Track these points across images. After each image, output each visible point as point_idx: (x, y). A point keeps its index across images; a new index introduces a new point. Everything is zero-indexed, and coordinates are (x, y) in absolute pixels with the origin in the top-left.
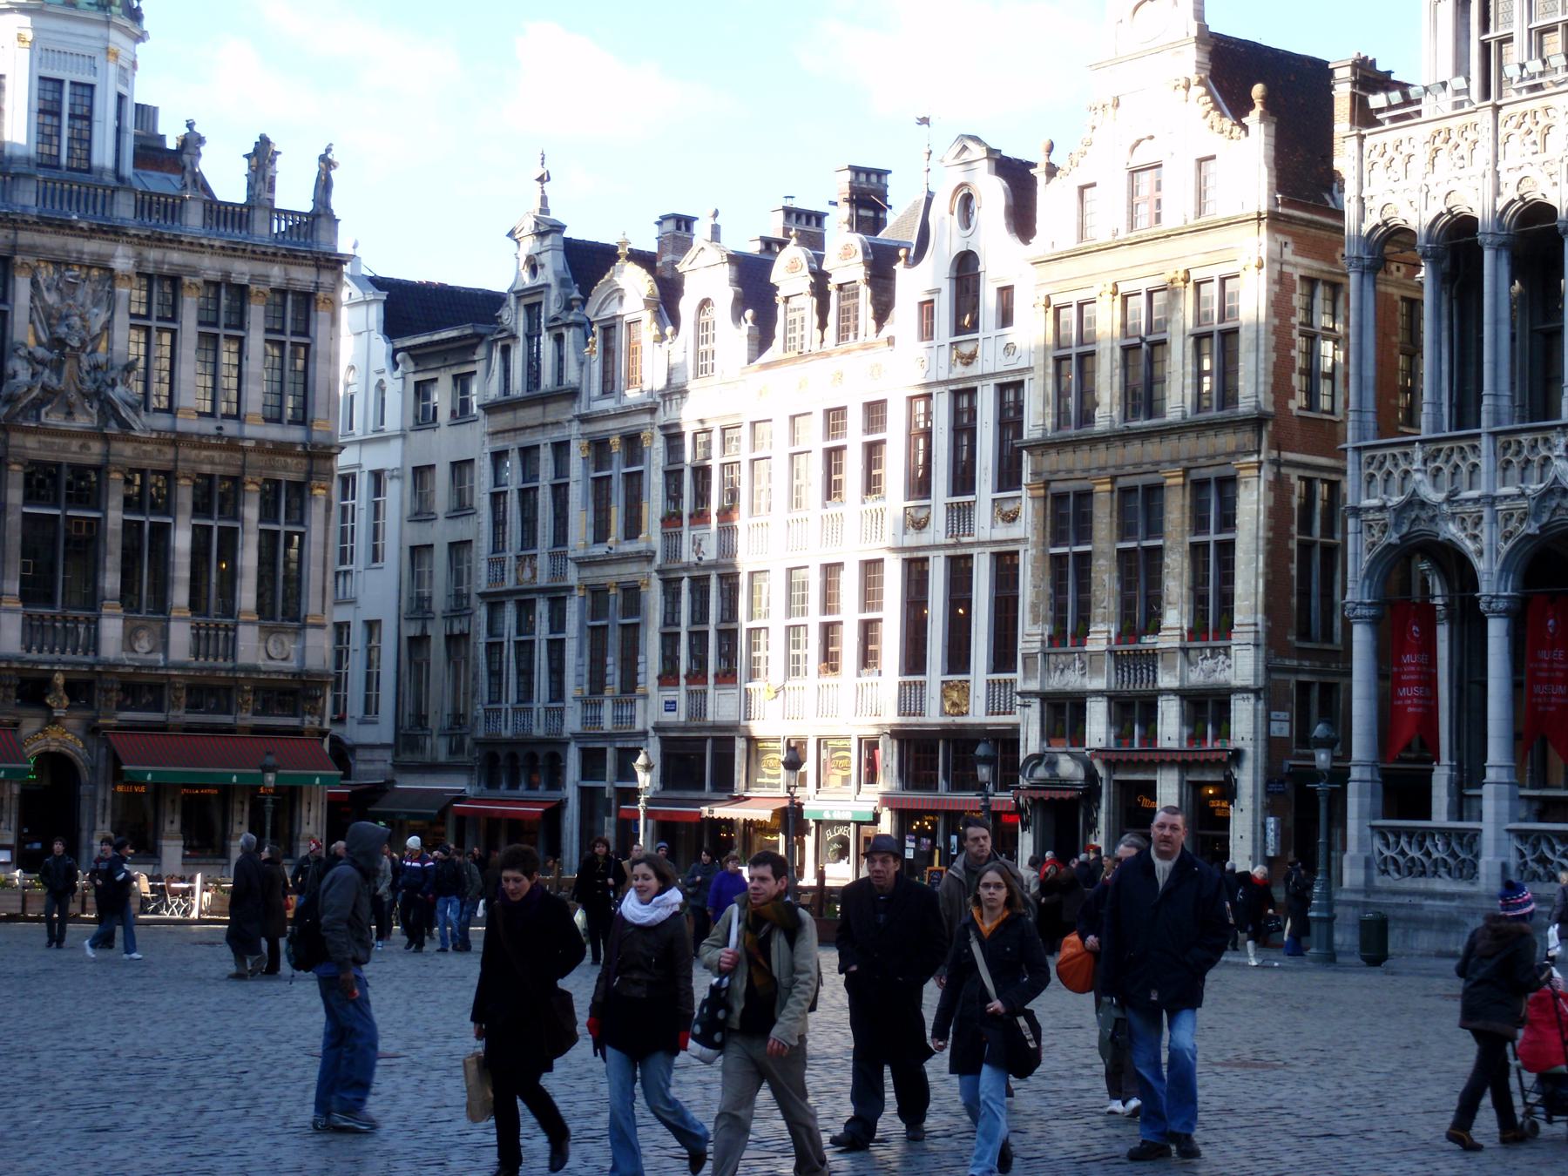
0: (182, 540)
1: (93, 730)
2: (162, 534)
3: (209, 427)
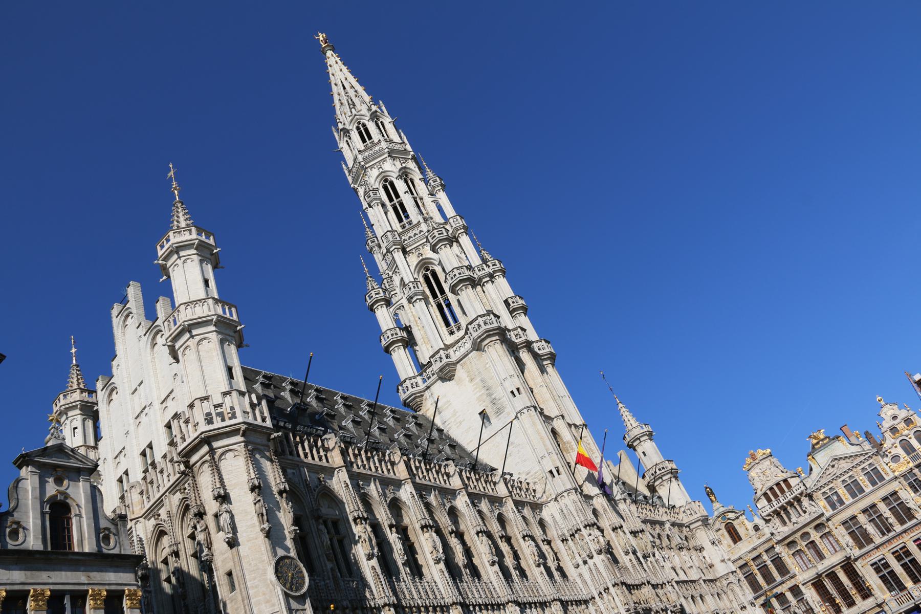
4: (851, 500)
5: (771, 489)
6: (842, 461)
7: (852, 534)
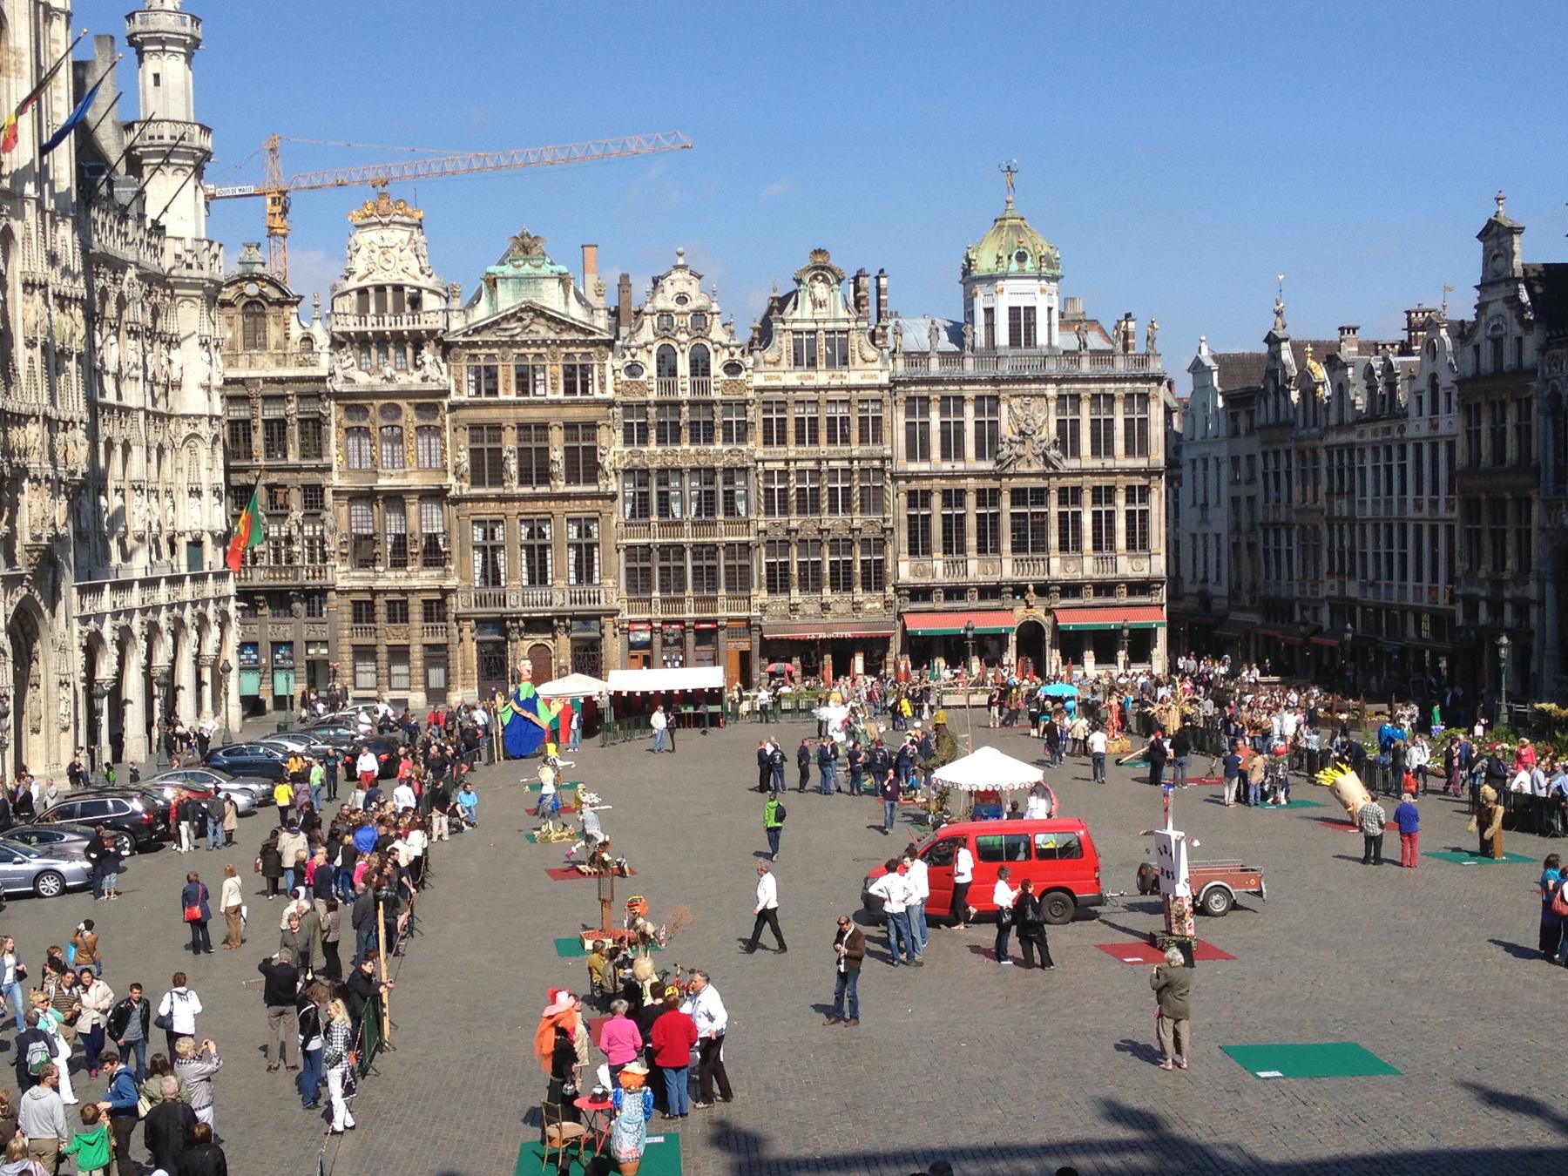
0: (1087, 519)
1: (1049, 612)
2: (1077, 515)
3: (1096, 464)
4: (513, 397)
5: (380, 289)
6: (542, 321)
7: (475, 454)
